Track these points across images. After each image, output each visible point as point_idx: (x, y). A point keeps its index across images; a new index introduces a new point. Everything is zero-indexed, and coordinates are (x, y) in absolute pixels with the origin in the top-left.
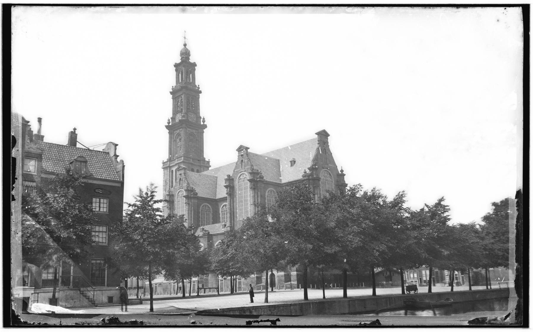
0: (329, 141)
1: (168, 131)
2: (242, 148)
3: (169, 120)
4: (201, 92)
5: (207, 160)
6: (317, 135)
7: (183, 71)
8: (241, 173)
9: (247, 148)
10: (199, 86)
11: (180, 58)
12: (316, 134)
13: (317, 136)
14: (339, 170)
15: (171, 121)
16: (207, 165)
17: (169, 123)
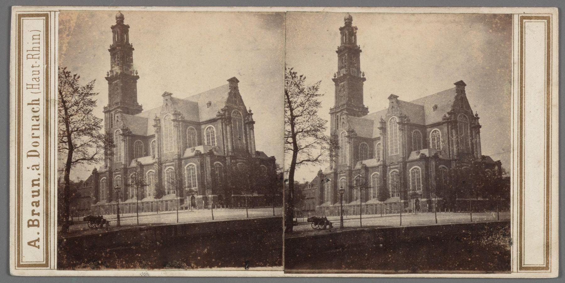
0: (239, 86)
1: (107, 82)
2: (166, 94)
3: (108, 73)
4: (133, 49)
6: (228, 82)
7: (119, 32)
8: (166, 115)
9: (171, 94)
10: (132, 44)
11: (116, 21)
12: (227, 80)
13: (228, 82)
14: (248, 109)
15: (109, 73)
16: (140, 109)
17: (108, 75)
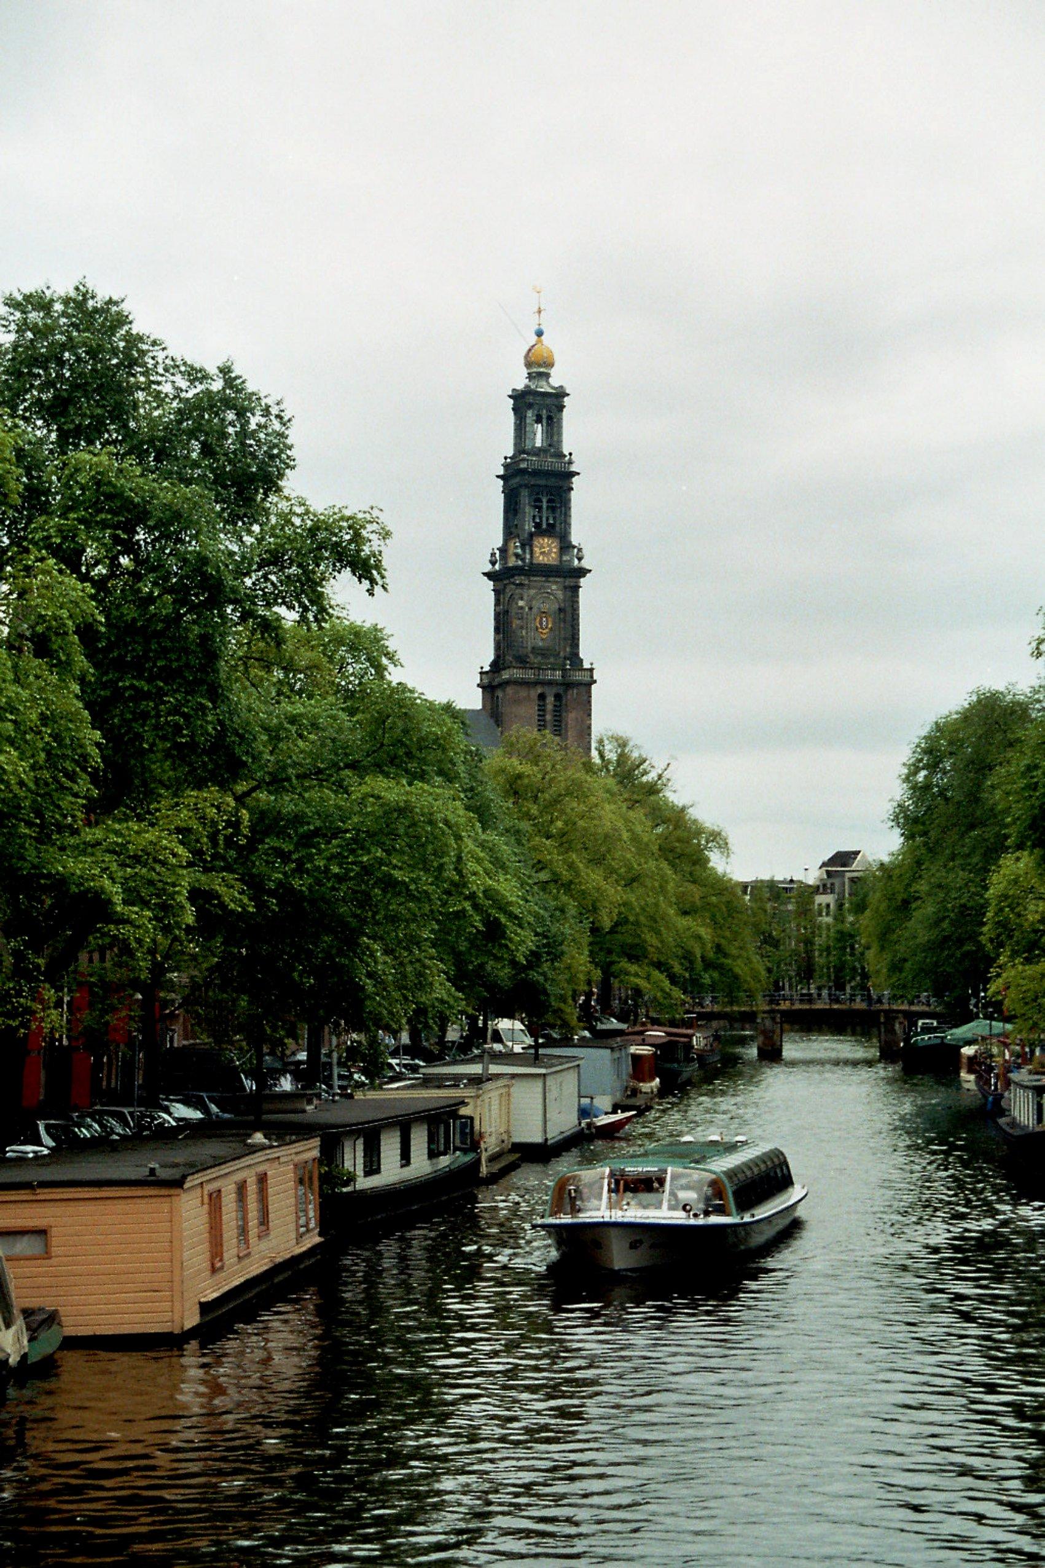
1: (491, 584)
5: (586, 665)
10: (570, 454)
15: (497, 555)
